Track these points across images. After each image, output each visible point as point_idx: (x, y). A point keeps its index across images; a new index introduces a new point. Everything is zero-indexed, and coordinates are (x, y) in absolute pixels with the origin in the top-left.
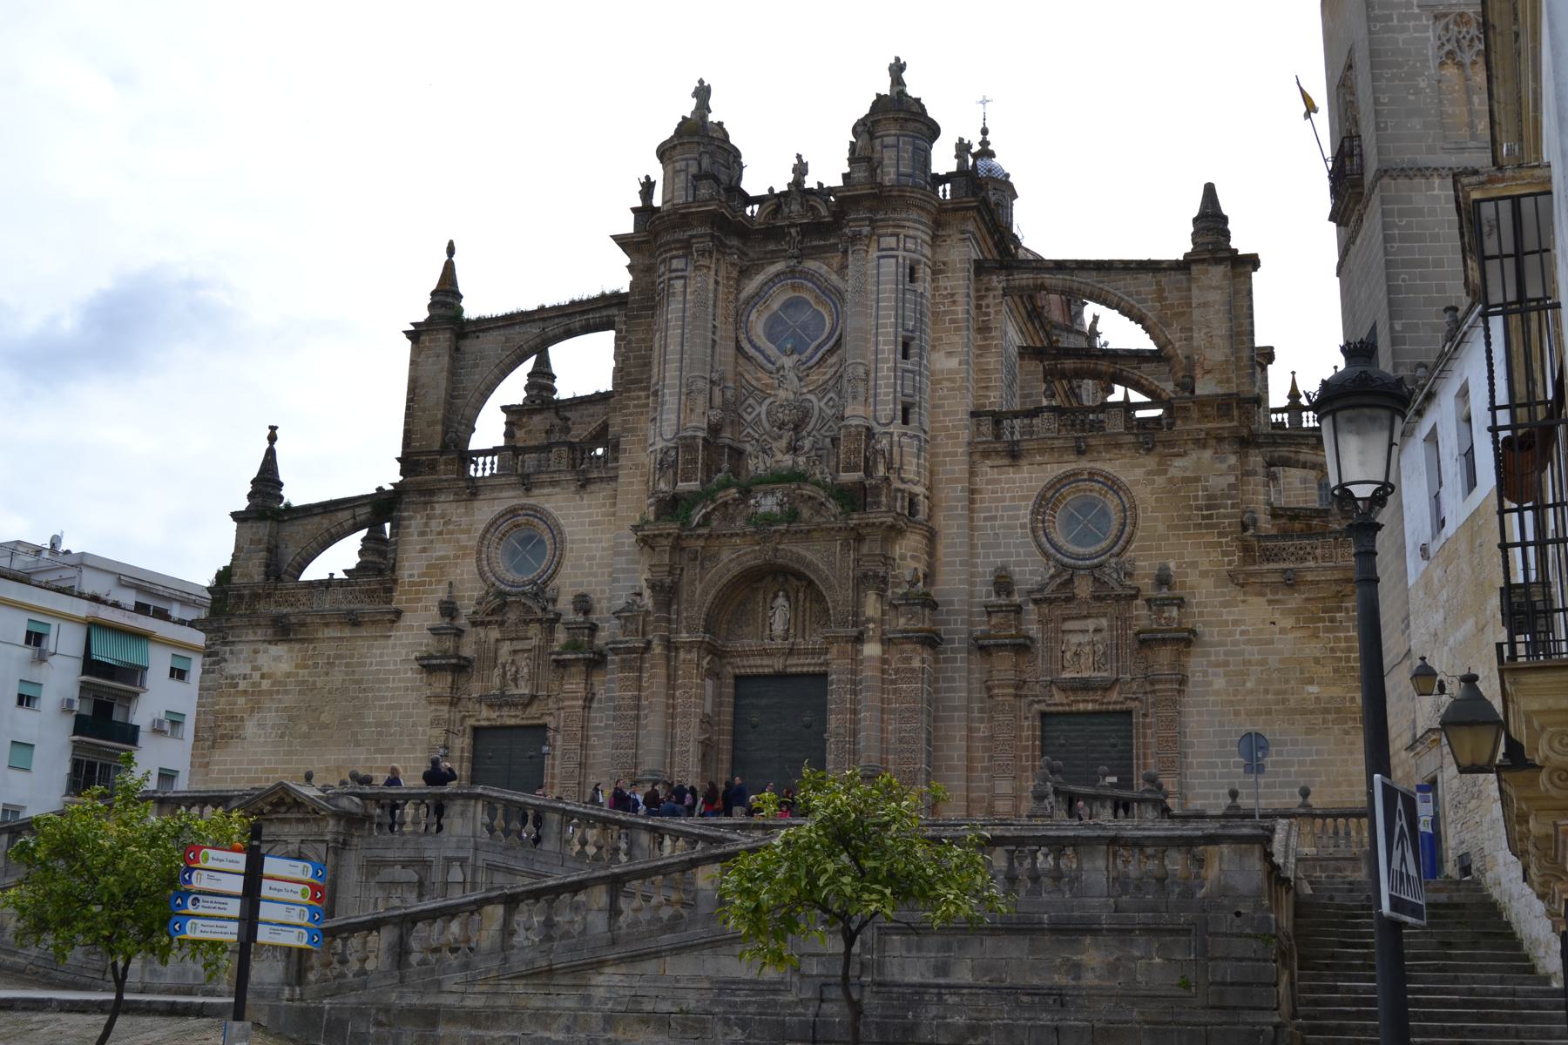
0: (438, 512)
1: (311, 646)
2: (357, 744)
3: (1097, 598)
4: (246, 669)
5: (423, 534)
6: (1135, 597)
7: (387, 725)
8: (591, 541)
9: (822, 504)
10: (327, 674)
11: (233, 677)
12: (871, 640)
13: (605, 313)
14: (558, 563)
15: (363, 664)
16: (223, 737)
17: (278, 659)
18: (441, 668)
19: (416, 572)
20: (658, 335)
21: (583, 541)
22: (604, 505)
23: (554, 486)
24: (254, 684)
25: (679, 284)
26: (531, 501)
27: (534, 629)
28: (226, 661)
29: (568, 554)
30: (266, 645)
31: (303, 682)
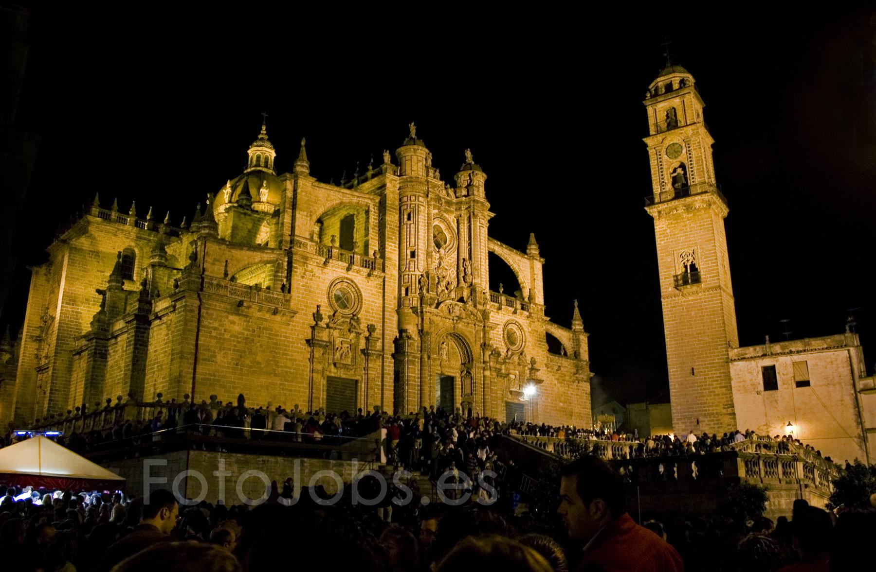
0: (310, 268)
1: (251, 320)
2: (275, 375)
3: (519, 364)
4: (216, 325)
5: (303, 277)
6: (525, 366)
7: (290, 368)
8: (372, 302)
9: (474, 315)
10: (259, 337)
11: (209, 328)
12: (487, 370)
13: (366, 201)
14: (361, 308)
15: (277, 335)
16: (204, 360)
17: (233, 323)
18: (320, 346)
19: (300, 295)
20: (413, 226)
21: (369, 301)
22: (377, 287)
23: (357, 273)
24: (220, 334)
25: (422, 208)
26: (349, 277)
27: (353, 335)
28: (204, 317)
29: (364, 306)
30: (225, 314)
31: (246, 339)
